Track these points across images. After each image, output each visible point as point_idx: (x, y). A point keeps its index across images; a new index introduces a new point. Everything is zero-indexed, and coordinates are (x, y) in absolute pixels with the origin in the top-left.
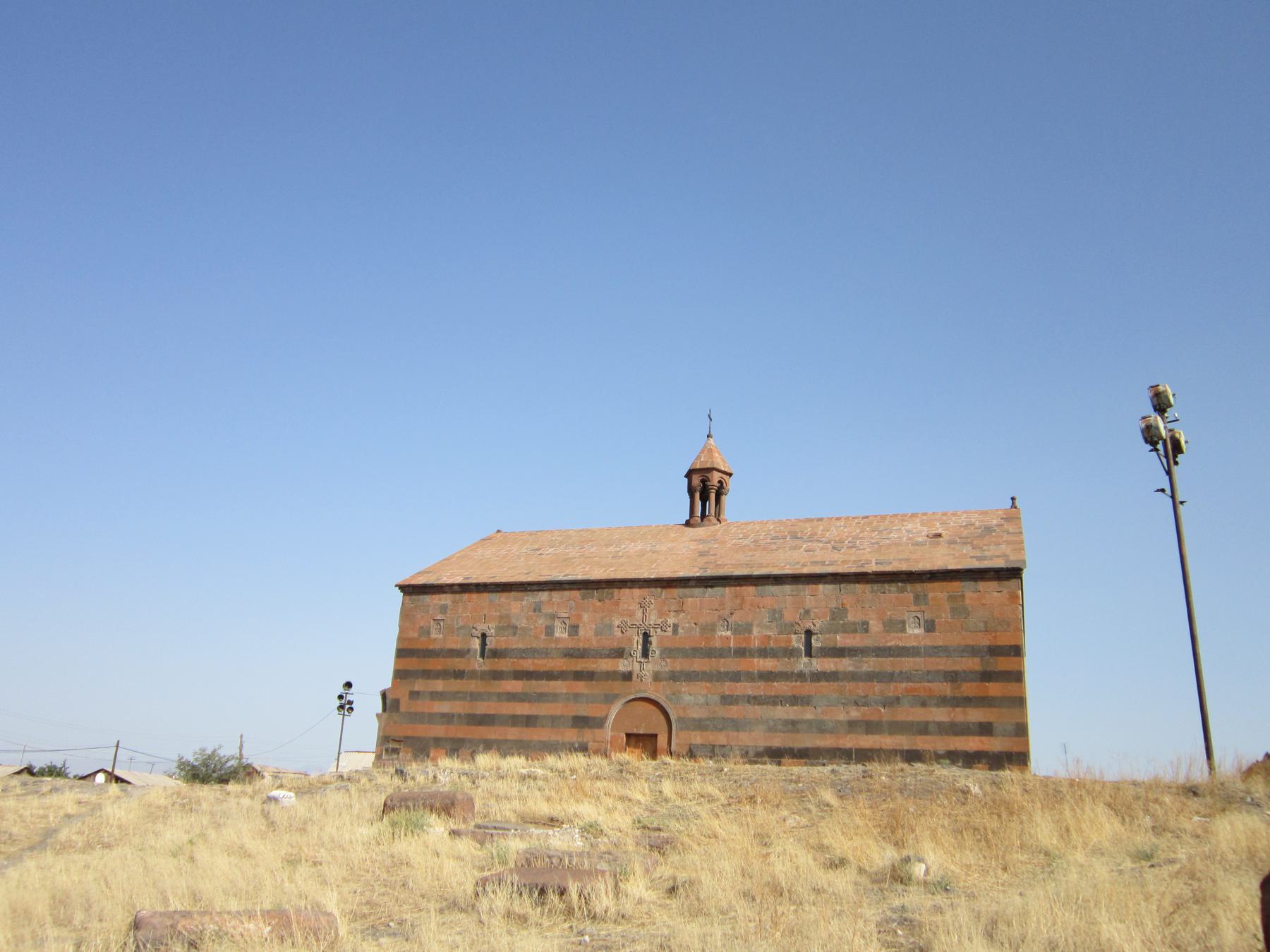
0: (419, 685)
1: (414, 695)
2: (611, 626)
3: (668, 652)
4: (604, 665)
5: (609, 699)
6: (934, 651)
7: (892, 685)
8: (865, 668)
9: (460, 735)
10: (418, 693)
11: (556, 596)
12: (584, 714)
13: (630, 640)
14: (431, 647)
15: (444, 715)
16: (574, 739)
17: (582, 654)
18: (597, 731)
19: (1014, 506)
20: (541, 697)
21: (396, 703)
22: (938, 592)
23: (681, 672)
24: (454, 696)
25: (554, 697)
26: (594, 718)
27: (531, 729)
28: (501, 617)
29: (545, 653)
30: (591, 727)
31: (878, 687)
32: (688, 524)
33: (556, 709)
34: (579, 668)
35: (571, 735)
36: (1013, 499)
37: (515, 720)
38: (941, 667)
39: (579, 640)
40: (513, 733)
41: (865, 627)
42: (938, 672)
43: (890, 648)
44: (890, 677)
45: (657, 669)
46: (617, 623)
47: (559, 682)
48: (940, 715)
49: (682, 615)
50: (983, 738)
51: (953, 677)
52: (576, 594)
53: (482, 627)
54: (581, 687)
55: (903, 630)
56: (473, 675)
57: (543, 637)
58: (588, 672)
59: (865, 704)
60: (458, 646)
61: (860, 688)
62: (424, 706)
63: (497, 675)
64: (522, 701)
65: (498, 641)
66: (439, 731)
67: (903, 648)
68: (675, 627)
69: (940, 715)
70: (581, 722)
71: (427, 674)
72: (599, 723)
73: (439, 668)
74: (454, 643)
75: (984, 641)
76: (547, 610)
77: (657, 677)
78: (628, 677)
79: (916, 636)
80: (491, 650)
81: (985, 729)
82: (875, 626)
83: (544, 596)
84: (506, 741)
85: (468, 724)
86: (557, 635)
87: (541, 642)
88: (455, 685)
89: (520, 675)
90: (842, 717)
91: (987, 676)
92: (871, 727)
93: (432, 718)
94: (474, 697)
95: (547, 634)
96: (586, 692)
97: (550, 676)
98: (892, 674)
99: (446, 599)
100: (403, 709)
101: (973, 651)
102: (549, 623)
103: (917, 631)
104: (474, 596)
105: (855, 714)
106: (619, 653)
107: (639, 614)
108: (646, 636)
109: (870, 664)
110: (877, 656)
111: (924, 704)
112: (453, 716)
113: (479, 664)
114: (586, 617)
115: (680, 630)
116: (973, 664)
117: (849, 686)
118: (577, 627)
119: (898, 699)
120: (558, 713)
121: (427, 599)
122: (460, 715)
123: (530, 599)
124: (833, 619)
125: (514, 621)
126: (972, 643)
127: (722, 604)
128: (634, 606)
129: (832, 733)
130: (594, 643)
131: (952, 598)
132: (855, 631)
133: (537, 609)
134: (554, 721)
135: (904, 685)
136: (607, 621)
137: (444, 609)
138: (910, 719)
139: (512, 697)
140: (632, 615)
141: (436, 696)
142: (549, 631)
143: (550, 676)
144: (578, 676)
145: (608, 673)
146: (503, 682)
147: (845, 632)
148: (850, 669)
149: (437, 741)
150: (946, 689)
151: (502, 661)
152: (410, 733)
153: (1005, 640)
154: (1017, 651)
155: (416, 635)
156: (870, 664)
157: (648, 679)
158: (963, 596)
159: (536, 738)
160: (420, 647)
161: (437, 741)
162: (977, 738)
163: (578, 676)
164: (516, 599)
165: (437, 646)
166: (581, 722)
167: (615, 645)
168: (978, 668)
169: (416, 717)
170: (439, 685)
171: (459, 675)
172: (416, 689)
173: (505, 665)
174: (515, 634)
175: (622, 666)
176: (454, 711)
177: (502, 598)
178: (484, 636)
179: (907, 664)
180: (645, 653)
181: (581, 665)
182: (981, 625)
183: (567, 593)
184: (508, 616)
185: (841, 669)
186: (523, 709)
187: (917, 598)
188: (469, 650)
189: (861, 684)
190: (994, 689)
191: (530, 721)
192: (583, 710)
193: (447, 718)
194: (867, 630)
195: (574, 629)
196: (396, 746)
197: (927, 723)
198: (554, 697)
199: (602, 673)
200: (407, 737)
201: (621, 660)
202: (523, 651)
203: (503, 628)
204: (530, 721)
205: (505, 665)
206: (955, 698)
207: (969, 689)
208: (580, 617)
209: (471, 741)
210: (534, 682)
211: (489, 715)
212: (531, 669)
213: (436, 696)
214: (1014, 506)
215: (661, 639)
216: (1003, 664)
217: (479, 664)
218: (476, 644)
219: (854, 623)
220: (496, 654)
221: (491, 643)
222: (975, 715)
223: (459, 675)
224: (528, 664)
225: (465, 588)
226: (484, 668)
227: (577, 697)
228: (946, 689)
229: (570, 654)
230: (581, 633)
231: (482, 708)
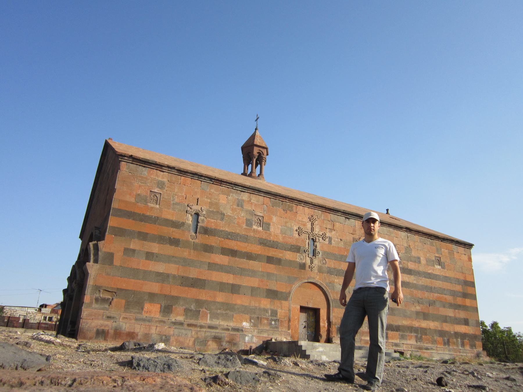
0: (134, 244)
1: (129, 252)
2: (291, 229)
3: (328, 255)
4: (288, 256)
5: (291, 281)
6: (446, 279)
7: (432, 294)
8: (420, 283)
9: (174, 293)
10: (134, 251)
11: (255, 199)
12: (275, 289)
13: (304, 242)
14: (148, 214)
15: (159, 274)
16: (268, 306)
17: (274, 245)
18: (283, 302)
19: (387, 213)
20: (242, 272)
21: (110, 257)
22: (445, 249)
23: (335, 269)
24: (169, 259)
25: (253, 273)
26: (282, 292)
27: (235, 295)
28: (211, 204)
29: (245, 239)
30: (279, 299)
31: (427, 294)
32: (244, 174)
33: (254, 282)
34: (270, 255)
35: (266, 303)
36: (387, 210)
37: (222, 287)
38: (449, 288)
39: (270, 234)
40: (221, 297)
41: (418, 260)
42: (448, 290)
43: (429, 274)
44: (430, 289)
45: (320, 264)
46: (295, 228)
47: (256, 263)
48: (450, 313)
49: (333, 232)
50: (466, 327)
51: (454, 293)
52: (267, 200)
53: (196, 208)
54: (271, 268)
55: (434, 266)
56: (187, 245)
57: (244, 226)
58: (277, 258)
59: (422, 303)
60: (174, 219)
61: (419, 294)
62: (140, 263)
63: (208, 249)
64: (228, 272)
65: (208, 222)
66: (154, 287)
67: (435, 275)
68: (330, 239)
69: (450, 313)
70: (273, 294)
71: (143, 236)
72: (285, 297)
73: (156, 233)
74: (169, 214)
75: (462, 278)
76: (247, 207)
77: (320, 270)
78: (303, 266)
79: (439, 269)
80: (202, 227)
81: (466, 322)
82: (423, 261)
83: (245, 196)
84: (215, 302)
85: (182, 284)
86: (255, 227)
87: (242, 230)
88: (169, 250)
89: (225, 251)
90: (413, 309)
91: (465, 295)
92: (426, 316)
93: (146, 275)
94: (186, 263)
95: (247, 225)
96: (275, 273)
97: (249, 256)
98: (431, 288)
99: (163, 176)
100: (117, 262)
101: (457, 281)
102: (249, 217)
103: (439, 267)
104: (188, 180)
105: (418, 308)
106: (296, 249)
107: (309, 225)
108: (314, 241)
109: (423, 281)
110: (425, 277)
111: (444, 307)
112: (168, 276)
113: (189, 235)
114: (274, 219)
115: (333, 242)
116: (458, 288)
117: (415, 292)
118: (269, 224)
119: (434, 302)
120: (256, 285)
121: (145, 171)
122: (174, 277)
123: (235, 196)
124: (406, 253)
125: (222, 209)
126: (458, 277)
127: (354, 231)
128: (306, 220)
129: (410, 318)
130: (281, 239)
131: (449, 253)
132: (415, 262)
133: (240, 204)
134: (254, 291)
135: (436, 295)
136: (289, 225)
137: (161, 185)
138: (440, 313)
139: (221, 268)
140: (305, 225)
141: (150, 256)
142: (249, 223)
143: (249, 256)
144: (270, 260)
145: (290, 261)
146: (213, 255)
147: (411, 261)
148: (415, 282)
149: (152, 297)
150: (449, 298)
151: (211, 238)
152: (124, 286)
153: (469, 279)
154: (472, 284)
155: (133, 200)
156: (423, 281)
157: (315, 270)
158: (453, 253)
159: (239, 302)
160: (137, 211)
161: (152, 297)
162: (464, 326)
163: (270, 260)
164: (223, 193)
165: (154, 214)
166: (273, 294)
167: (294, 243)
168: (461, 291)
169: (135, 273)
170: (155, 248)
171: (175, 242)
172: (132, 247)
173: (213, 241)
174: (222, 219)
175: (299, 258)
176: (169, 272)
177: (214, 189)
178: (197, 214)
179: (438, 284)
180: (314, 253)
181: (272, 253)
182: (460, 269)
183: (261, 198)
184: (217, 204)
185: (411, 281)
186: (229, 279)
187: (437, 249)
188: (183, 224)
189: (419, 291)
190: (468, 302)
191: (234, 289)
192: (274, 287)
193: (162, 277)
194: (420, 262)
195: (266, 226)
196: (108, 296)
197: (446, 316)
198: (253, 273)
199: (286, 260)
200: (121, 290)
201: (298, 254)
202: (229, 233)
203: (213, 212)
204: (234, 289)
205: (213, 241)
206: (455, 304)
207: (459, 301)
208: (271, 219)
209: (185, 299)
210: (237, 259)
211: (200, 279)
212: (236, 248)
213: (150, 256)
214: (387, 213)
215: (322, 247)
216: (469, 290)
217: (189, 235)
218: (190, 220)
219: (415, 257)
220: (206, 231)
221: (203, 222)
222: (462, 315)
223: (175, 242)
224: (233, 245)
225: (182, 172)
226: (197, 241)
227: (269, 275)
228: (449, 298)
229: (264, 243)
230: (272, 229)
231: (193, 273)
